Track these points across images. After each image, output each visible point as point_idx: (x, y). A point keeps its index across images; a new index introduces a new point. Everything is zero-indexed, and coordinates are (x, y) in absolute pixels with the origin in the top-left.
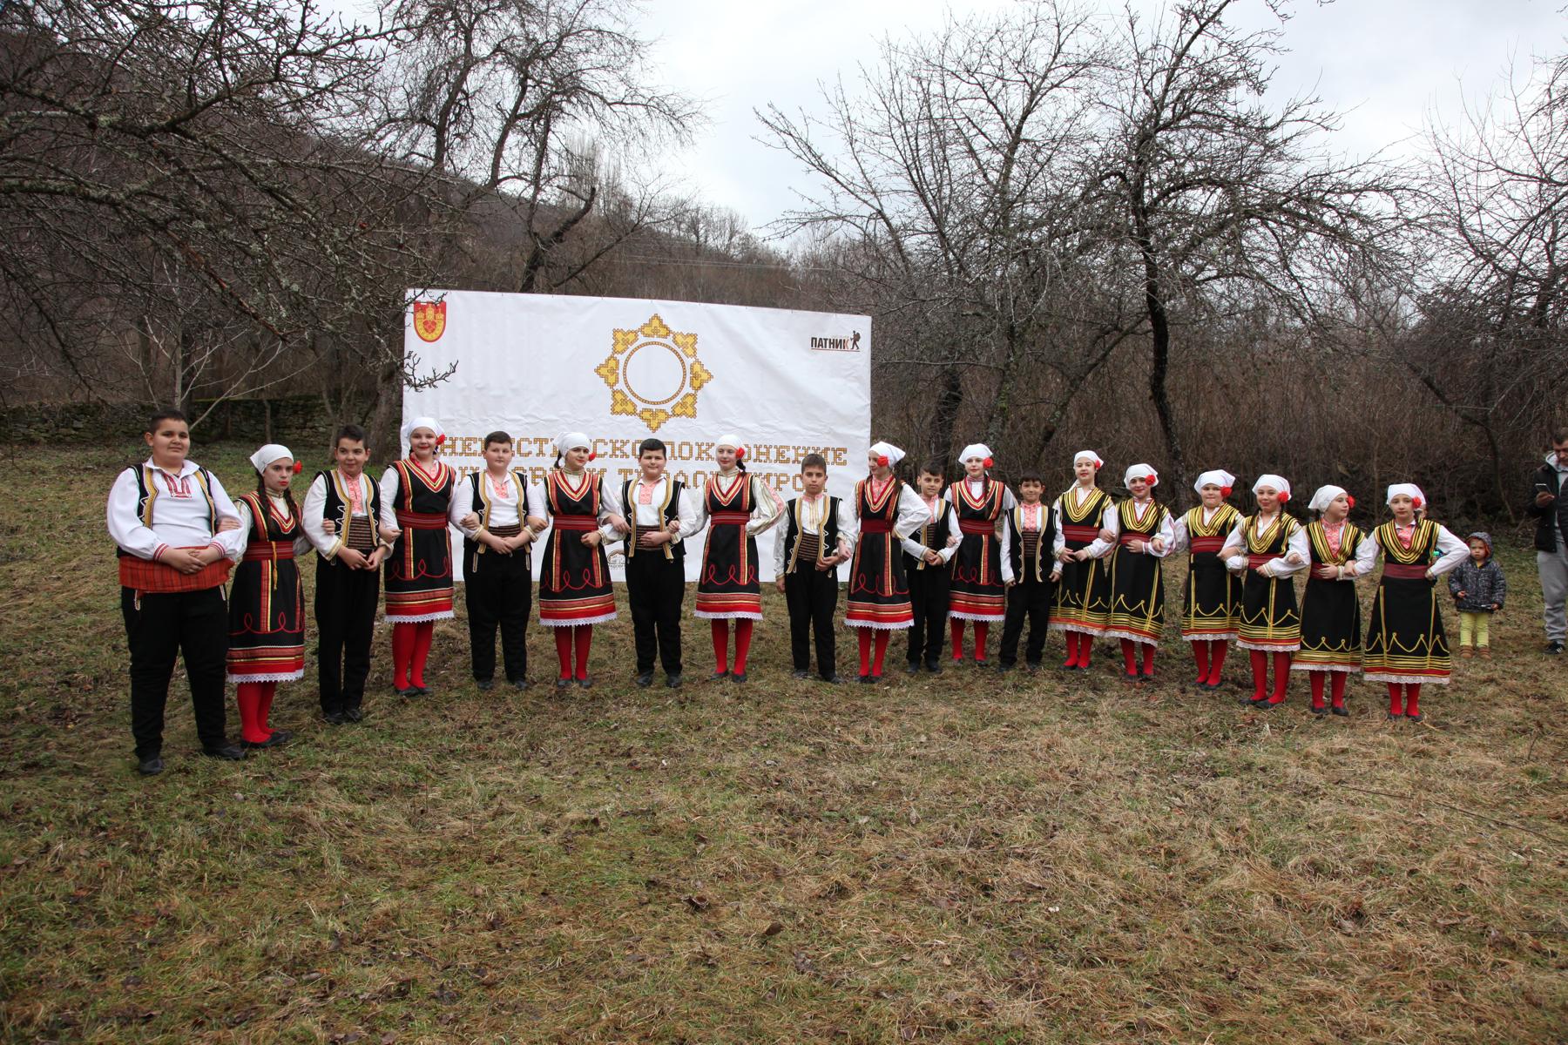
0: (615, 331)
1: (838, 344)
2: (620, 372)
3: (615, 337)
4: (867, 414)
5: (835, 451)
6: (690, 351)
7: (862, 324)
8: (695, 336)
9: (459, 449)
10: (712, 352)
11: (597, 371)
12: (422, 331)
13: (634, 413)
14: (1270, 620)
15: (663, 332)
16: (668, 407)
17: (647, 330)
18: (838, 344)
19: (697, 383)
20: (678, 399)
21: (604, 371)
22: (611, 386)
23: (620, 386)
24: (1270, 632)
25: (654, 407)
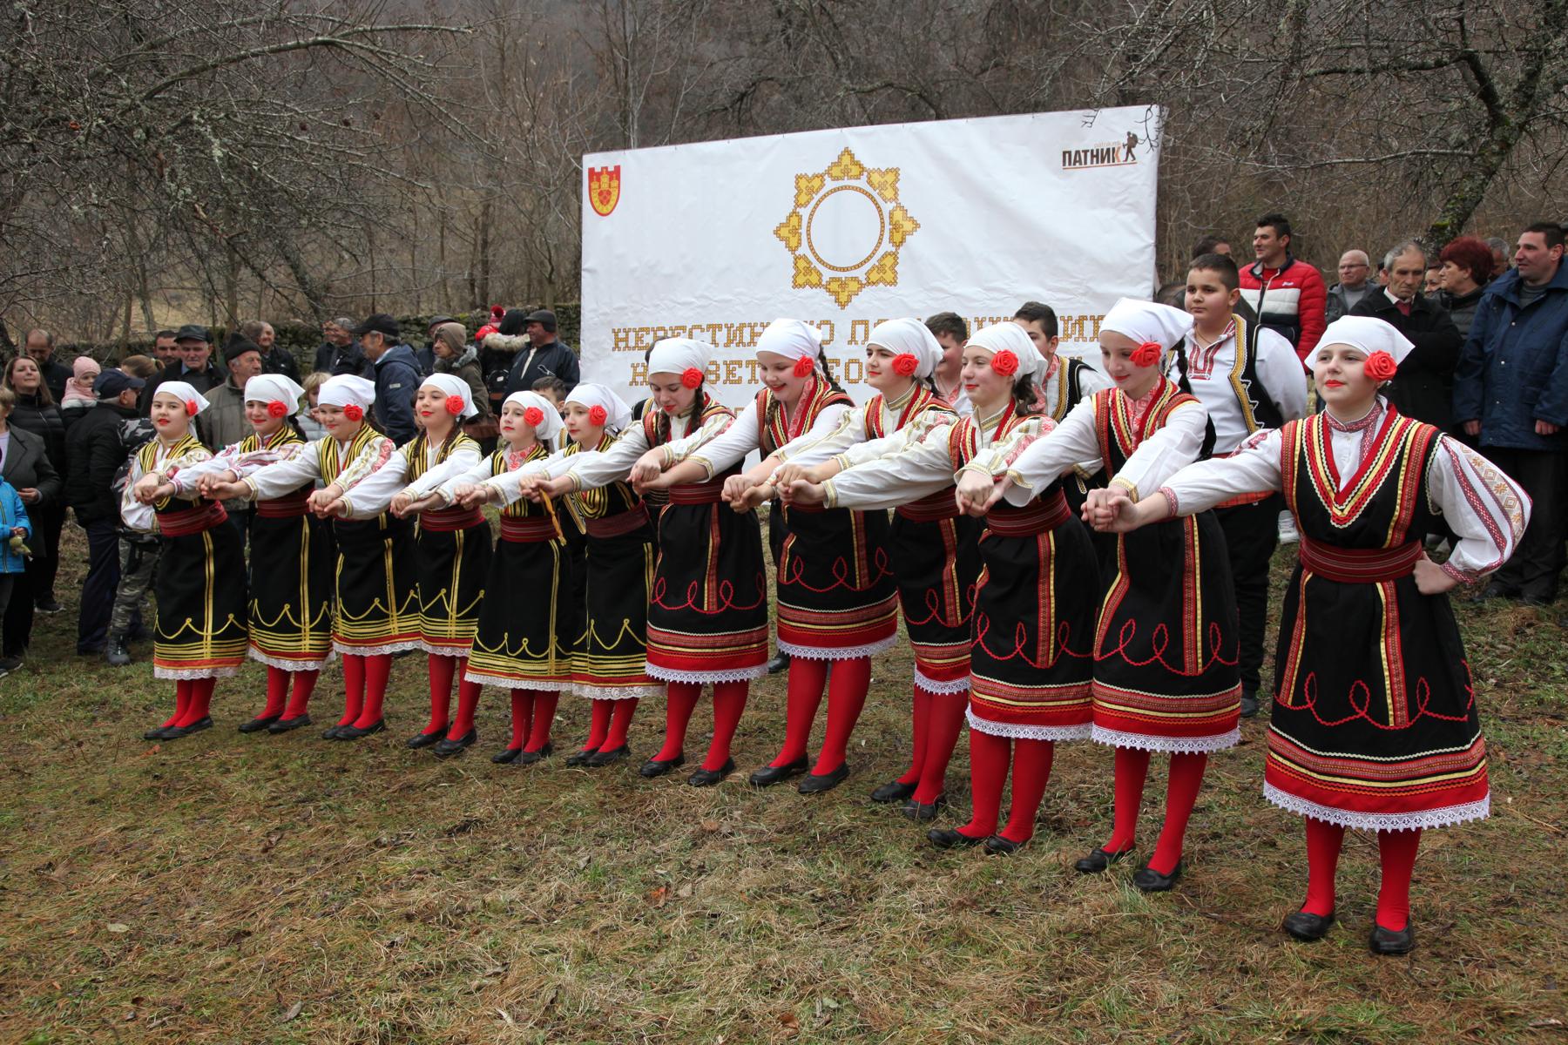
0: (798, 178)
1: (1104, 156)
4: (1148, 259)
5: (741, 342)
6: (889, 193)
7: (1142, 120)
8: (896, 171)
9: (632, 343)
10: (923, 192)
12: (597, 204)
13: (819, 285)
14: (452, 608)
15: (855, 170)
16: (860, 274)
18: (1104, 156)
19: (897, 238)
20: (874, 261)
21: (784, 232)
22: (793, 250)
23: (804, 250)
24: (452, 628)
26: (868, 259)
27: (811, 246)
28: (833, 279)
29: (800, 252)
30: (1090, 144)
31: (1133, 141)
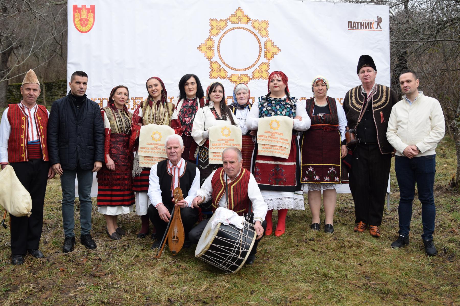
1: (366, 26)
2: (216, 48)
3: (211, 25)
6: (264, 33)
8: (267, 22)
11: (199, 48)
15: (245, 20)
16: (249, 73)
17: (234, 19)
18: (366, 26)
19: (269, 55)
20: (256, 67)
22: (209, 59)
23: (216, 58)
25: (239, 73)
26: (253, 65)
27: (220, 57)
28: (233, 75)
29: (214, 59)
30: (360, 19)
31: (380, 21)
